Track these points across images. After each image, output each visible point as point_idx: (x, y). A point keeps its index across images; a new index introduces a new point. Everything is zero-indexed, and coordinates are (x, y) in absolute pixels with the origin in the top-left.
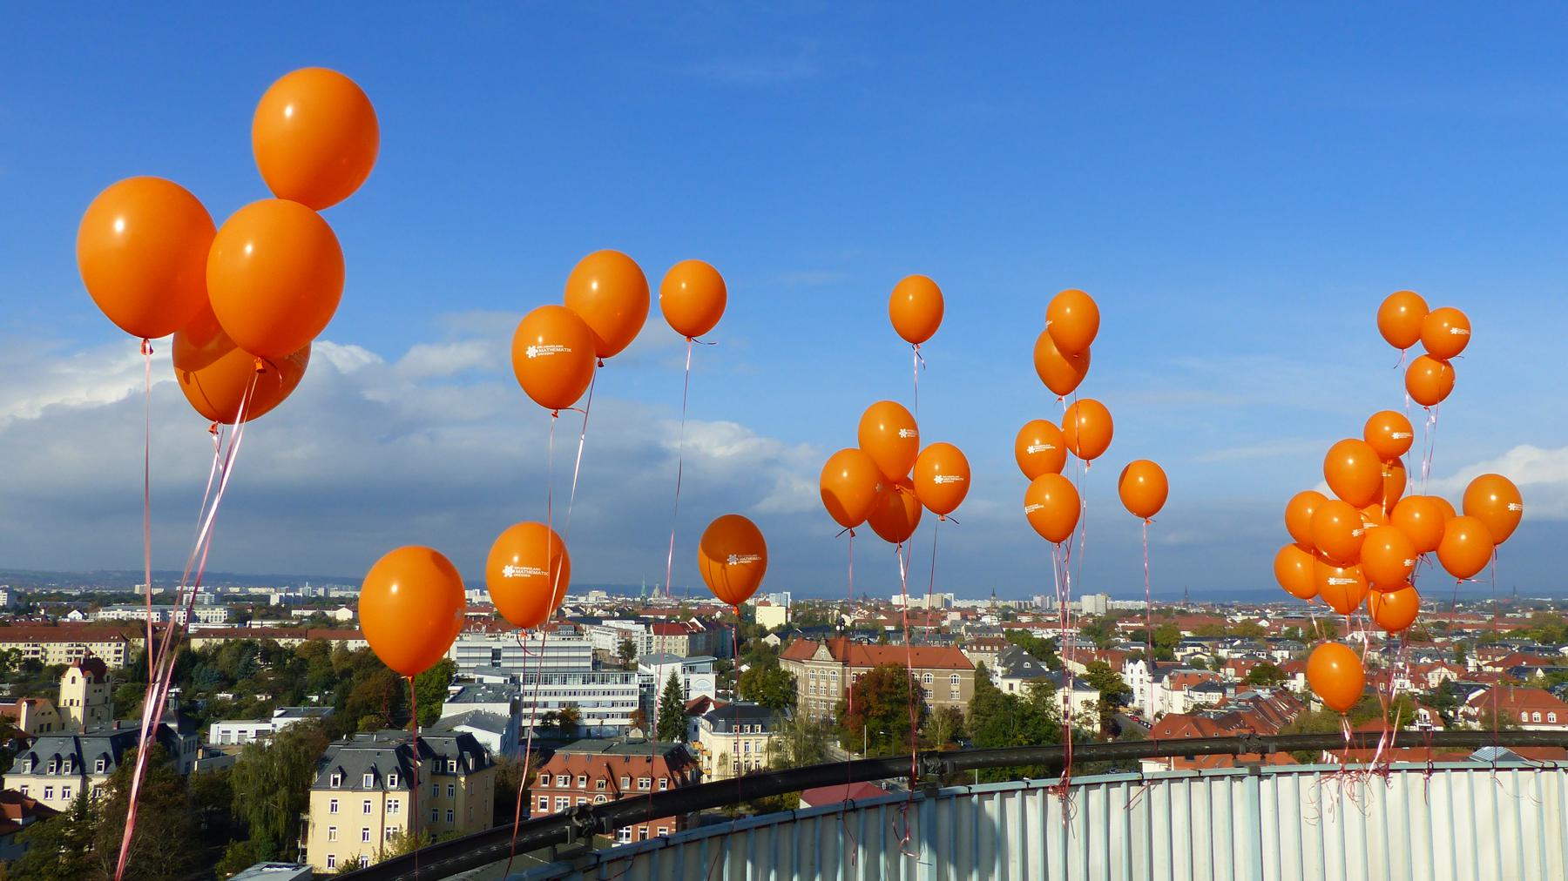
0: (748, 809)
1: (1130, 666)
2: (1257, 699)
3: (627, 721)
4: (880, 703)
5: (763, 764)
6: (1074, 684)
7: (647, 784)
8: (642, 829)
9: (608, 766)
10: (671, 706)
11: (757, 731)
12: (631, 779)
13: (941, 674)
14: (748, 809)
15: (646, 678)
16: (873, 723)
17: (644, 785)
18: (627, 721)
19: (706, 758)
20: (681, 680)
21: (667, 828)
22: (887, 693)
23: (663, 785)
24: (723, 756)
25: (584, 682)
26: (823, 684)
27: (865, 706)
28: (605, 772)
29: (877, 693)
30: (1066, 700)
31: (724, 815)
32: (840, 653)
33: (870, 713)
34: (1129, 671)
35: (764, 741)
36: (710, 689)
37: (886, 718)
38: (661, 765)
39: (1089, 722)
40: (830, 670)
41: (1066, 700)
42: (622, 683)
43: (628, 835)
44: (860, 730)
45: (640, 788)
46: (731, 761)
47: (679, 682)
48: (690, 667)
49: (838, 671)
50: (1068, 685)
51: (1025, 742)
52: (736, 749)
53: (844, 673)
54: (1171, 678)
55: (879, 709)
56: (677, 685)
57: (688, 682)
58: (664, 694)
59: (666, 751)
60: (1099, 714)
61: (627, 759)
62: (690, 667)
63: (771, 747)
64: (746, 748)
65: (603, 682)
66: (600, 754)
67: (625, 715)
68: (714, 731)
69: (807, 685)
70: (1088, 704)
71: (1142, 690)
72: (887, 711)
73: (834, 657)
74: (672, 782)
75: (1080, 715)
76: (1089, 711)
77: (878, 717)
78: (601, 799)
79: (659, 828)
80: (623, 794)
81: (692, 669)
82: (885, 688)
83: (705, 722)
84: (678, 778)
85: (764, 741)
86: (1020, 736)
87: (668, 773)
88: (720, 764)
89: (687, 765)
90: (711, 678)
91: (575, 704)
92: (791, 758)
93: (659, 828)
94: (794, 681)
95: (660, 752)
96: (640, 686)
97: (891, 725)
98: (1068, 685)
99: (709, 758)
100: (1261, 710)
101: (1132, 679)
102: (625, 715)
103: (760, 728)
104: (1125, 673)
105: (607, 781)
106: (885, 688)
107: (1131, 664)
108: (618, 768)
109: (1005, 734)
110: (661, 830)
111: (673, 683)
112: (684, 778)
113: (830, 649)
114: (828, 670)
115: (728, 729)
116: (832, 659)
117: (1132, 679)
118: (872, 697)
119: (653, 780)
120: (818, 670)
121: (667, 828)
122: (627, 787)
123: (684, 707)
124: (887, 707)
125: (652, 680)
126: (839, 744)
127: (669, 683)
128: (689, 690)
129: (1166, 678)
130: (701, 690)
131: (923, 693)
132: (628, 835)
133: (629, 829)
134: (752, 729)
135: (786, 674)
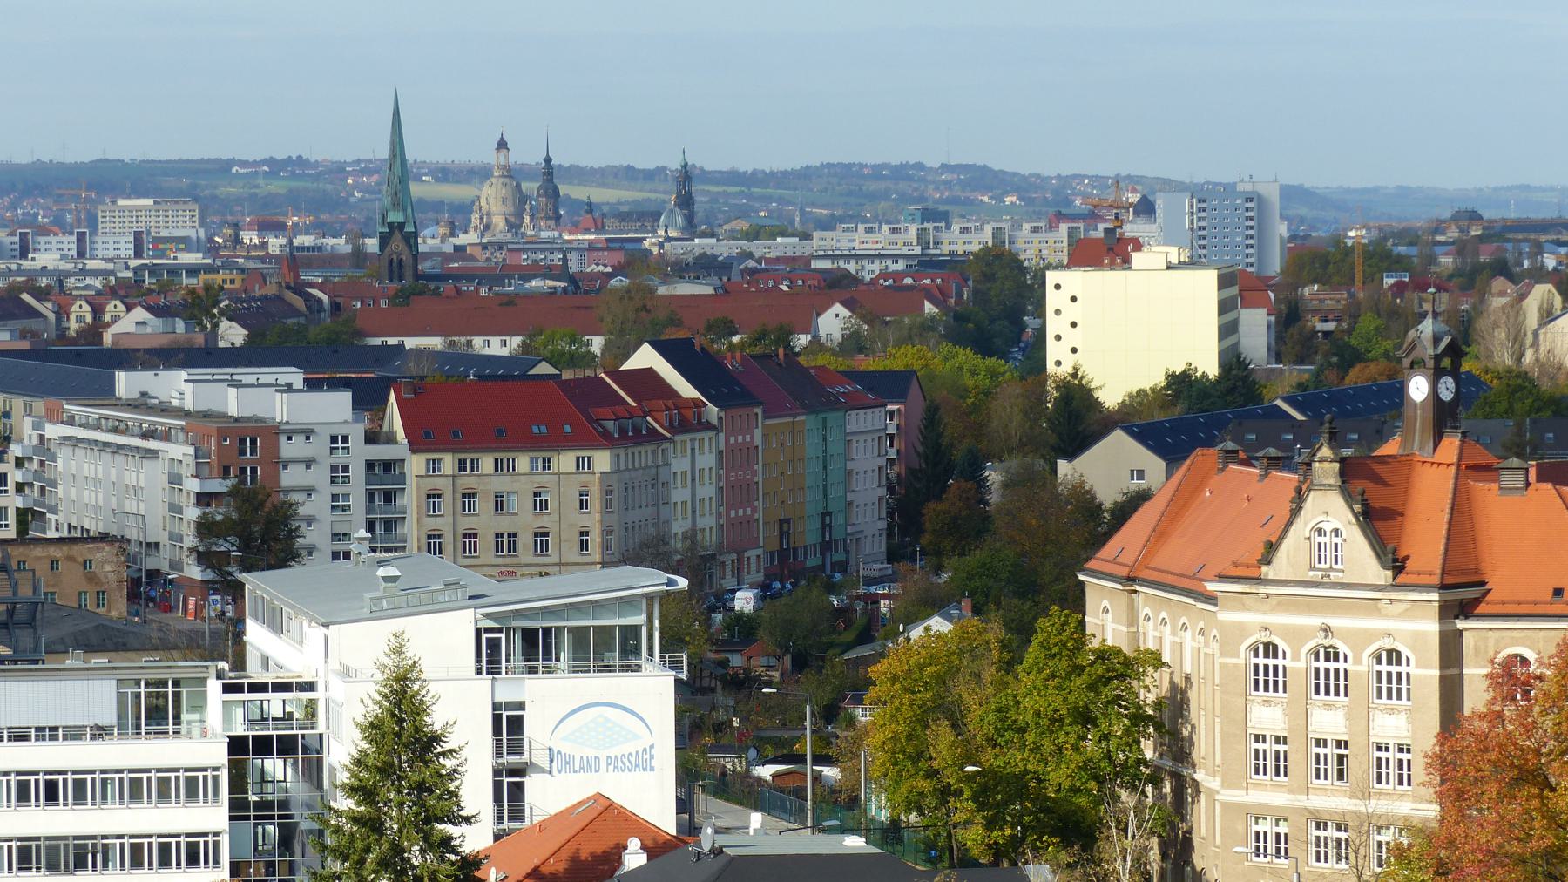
15: (275, 704)
36: (642, 762)
40: (1372, 635)
47: (436, 720)
48: (529, 636)
49: (1417, 639)
53: (1451, 652)
56: (425, 744)
57: (516, 725)
58: (352, 790)
62: (529, 636)
94: (1176, 704)
96: (237, 746)
101: (583, 504)
116: (1384, 576)
117: (583, 504)
120: (1287, 632)
125: (311, 709)
127: (373, 730)
128: (519, 771)
130: (590, 765)
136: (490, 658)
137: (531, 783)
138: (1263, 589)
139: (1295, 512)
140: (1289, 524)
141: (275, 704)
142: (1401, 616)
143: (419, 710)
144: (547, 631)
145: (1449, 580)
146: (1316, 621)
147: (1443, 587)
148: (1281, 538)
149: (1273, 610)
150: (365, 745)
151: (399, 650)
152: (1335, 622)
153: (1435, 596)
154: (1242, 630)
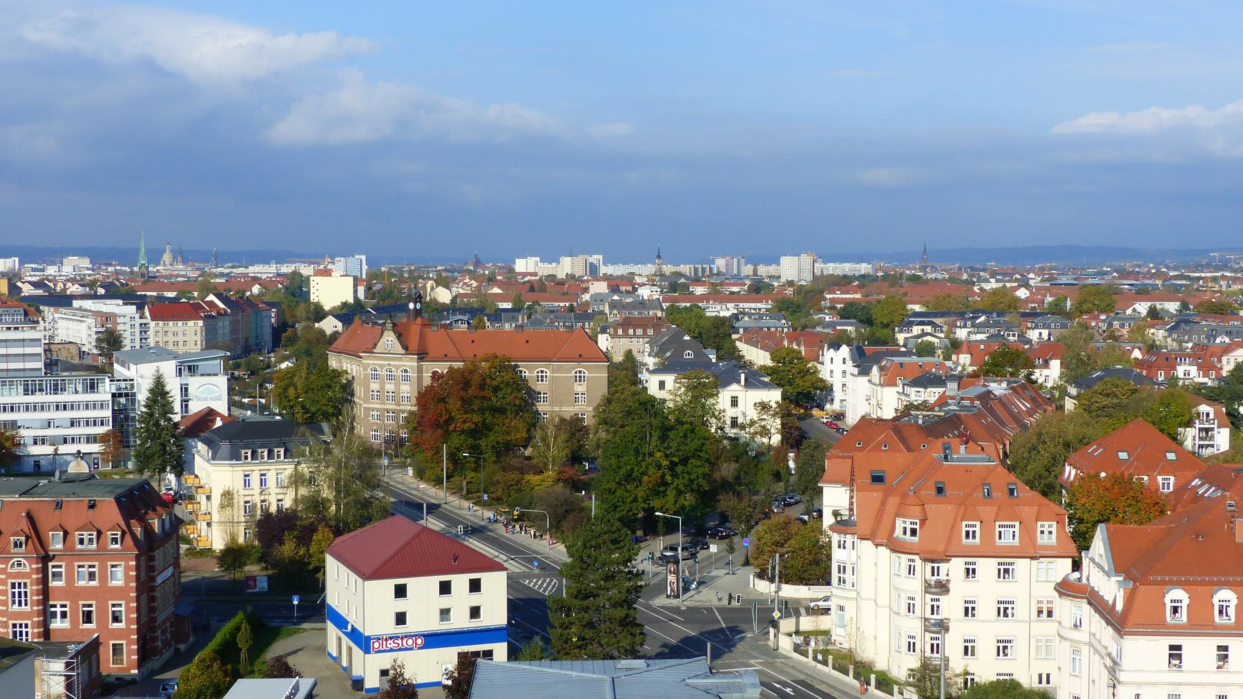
0: (262, 569)
1: (829, 354)
2: (986, 397)
3: (95, 448)
4: (466, 413)
5: (287, 503)
6: (746, 380)
7: (91, 541)
8: (84, 606)
9: (30, 516)
10: (157, 424)
11: (279, 456)
12: (66, 534)
13: (559, 370)
14: (262, 569)
15: (123, 385)
16: (456, 440)
17: (86, 541)
18: (95, 448)
19: (204, 497)
20: (173, 386)
21: (123, 602)
22: (476, 397)
23: (115, 540)
24: (228, 496)
25: (26, 392)
26: (390, 387)
27: (444, 418)
28: (25, 525)
29: (462, 399)
30: (734, 402)
31: (227, 578)
32: (414, 343)
33: (451, 428)
34: (827, 359)
35: (289, 469)
36: (219, 398)
37: (476, 432)
38: (110, 512)
39: (765, 432)
40: (401, 366)
41: (734, 402)
42: (85, 391)
43: (64, 615)
44: (438, 451)
45: (79, 547)
46: (239, 501)
47: (167, 389)
48: (190, 367)
49: (411, 367)
50: (738, 382)
51: (665, 463)
52: (247, 484)
54: (881, 369)
55: (465, 422)
56: (164, 394)
57: (186, 389)
59: (120, 491)
60: (778, 421)
61: (59, 505)
62: (190, 367)
63: (297, 480)
64: (263, 483)
65: (56, 391)
66: (16, 498)
67: (90, 439)
68: (214, 459)
69: (367, 388)
70: (764, 407)
71: (844, 385)
72: (476, 424)
73: (406, 347)
74: (128, 536)
75: (752, 423)
76: (764, 417)
77: (463, 432)
78: (19, 565)
79: (110, 603)
80: (54, 556)
81: (192, 370)
82: (471, 392)
83: (201, 446)
84: (138, 530)
85: (289, 469)
86: (658, 455)
87: (122, 523)
88: (222, 507)
89: (154, 510)
90: (222, 382)
91: (14, 425)
92: (327, 493)
93: (110, 603)
94: (350, 383)
95: (110, 492)
96: (114, 395)
97: (483, 443)
98: (738, 382)
99: (209, 498)
100: (991, 411)
102: (90, 439)
103: (282, 453)
104: (822, 363)
105: (27, 538)
106: (471, 392)
107: (832, 350)
108: (45, 519)
109: (637, 452)
110: (113, 606)
111: (159, 391)
112: (148, 530)
113: (399, 336)
114: (397, 367)
115: (235, 456)
116: (403, 351)
118: (454, 404)
119: (99, 533)
120: (382, 366)
121: (123, 602)
122: (60, 546)
123: (176, 425)
124: (476, 418)
125: (132, 386)
126: (410, 471)
127: (151, 391)
129: (875, 369)
130: (205, 399)
131: (533, 395)
132: (64, 615)
133: (64, 606)
134: (270, 455)
135: (337, 374)
136: (180, 373)
137: (190, 403)
138: (374, 355)
139: (381, 336)
140: (380, 339)
141: (123, 385)
142: (408, 361)
143: (163, 386)
144: (194, 366)
145: (419, 352)
146: (387, 363)
147: (417, 354)
148: (378, 342)
149: (376, 360)
150: (149, 395)
151: (158, 371)
152: (391, 363)
153: (416, 356)
154: (368, 365)
